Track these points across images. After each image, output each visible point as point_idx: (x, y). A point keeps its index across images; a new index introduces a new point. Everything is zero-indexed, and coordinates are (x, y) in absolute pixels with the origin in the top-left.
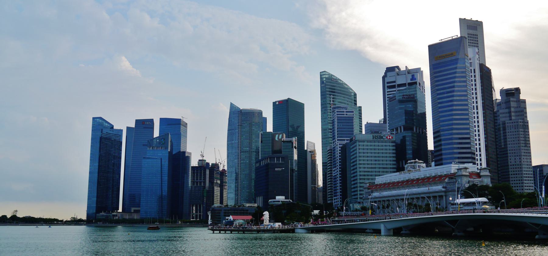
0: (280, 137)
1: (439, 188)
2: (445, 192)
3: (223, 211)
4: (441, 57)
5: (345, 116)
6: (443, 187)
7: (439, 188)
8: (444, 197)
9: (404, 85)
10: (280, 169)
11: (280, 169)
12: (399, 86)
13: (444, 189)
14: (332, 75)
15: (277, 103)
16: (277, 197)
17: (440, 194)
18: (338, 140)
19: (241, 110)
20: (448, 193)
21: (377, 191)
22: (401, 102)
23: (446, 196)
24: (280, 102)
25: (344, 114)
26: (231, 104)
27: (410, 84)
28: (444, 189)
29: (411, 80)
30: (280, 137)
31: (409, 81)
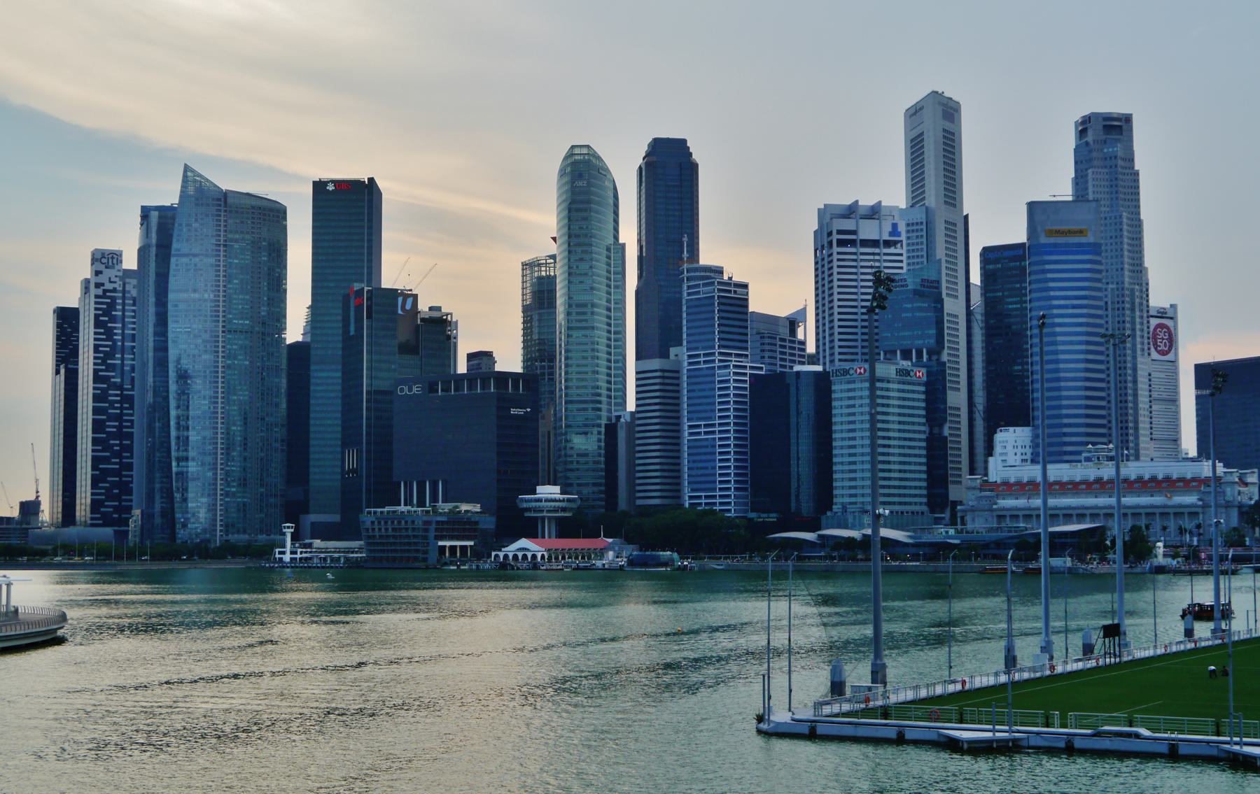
0: (408, 306)
1: (1190, 499)
2: (1203, 507)
3: (434, 526)
4: (1059, 233)
6: (1200, 500)
7: (1190, 499)
9: (875, 243)
10: (520, 412)
11: (520, 412)
12: (865, 243)
15: (331, 187)
16: (540, 489)
17: (1193, 510)
18: (720, 354)
19: (226, 195)
22: (916, 292)
24: (339, 184)
25: (730, 291)
26: (187, 169)
27: (888, 244)
29: (891, 234)
30: (408, 306)
31: (886, 237)
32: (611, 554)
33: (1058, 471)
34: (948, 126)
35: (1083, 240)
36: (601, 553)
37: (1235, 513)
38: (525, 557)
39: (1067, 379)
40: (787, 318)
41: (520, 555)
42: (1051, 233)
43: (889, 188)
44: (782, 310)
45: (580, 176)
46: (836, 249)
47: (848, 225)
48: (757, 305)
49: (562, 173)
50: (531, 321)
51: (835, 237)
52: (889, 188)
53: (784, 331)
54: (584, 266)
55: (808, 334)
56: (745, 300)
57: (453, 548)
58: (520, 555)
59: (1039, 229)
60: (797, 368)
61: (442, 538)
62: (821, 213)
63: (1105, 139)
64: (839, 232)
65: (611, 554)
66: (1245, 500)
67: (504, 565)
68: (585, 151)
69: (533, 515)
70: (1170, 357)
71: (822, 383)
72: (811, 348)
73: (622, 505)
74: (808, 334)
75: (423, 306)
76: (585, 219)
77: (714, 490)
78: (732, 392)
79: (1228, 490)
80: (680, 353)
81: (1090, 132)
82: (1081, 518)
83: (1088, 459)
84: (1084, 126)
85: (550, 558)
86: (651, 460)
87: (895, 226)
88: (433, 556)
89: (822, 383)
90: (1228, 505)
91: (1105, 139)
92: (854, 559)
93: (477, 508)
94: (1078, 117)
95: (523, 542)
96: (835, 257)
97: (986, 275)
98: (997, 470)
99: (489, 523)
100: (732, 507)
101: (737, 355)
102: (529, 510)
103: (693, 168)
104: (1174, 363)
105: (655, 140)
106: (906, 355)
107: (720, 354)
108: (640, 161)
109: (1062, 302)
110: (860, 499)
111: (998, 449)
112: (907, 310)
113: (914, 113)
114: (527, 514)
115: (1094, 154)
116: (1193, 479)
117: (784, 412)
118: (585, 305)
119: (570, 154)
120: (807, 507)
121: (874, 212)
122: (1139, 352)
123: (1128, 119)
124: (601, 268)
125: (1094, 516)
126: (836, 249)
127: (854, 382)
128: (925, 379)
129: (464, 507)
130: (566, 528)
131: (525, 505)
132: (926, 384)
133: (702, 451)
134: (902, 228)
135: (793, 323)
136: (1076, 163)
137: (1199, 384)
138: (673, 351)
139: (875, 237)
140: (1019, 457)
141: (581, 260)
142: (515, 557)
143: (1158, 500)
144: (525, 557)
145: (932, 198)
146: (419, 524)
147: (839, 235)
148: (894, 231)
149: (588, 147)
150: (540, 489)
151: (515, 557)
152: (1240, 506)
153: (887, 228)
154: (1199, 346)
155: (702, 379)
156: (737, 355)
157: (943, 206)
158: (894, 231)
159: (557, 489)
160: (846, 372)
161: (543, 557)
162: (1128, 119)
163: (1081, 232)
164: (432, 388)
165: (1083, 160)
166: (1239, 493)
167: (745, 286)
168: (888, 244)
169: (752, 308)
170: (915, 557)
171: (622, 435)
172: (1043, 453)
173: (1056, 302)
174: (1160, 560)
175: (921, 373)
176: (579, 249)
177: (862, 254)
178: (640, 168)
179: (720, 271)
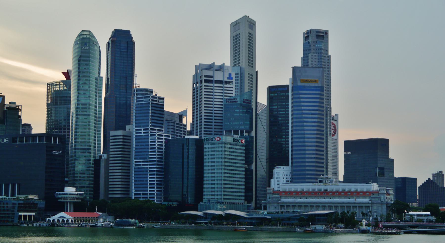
2: (371, 204)
3: (17, 206)
4: (306, 81)
5: (157, 103)
6: (370, 201)
7: (366, 200)
8: (370, 208)
9: (221, 82)
12: (217, 82)
13: (370, 202)
14: (94, 37)
16: (66, 189)
18: (151, 129)
20: (373, 205)
21: (286, 197)
22: (241, 105)
23: (371, 206)
25: (156, 101)
27: (227, 82)
28: (370, 202)
29: (228, 78)
31: (226, 79)
32: (101, 220)
33: (299, 187)
34: (251, 31)
35: (316, 85)
36: (97, 219)
37: (385, 207)
38: (63, 221)
39: (308, 146)
40: (179, 114)
41: (61, 219)
42: (302, 81)
43: (223, 57)
44: (177, 111)
45: (86, 45)
46: (204, 84)
47: (210, 73)
48: (167, 108)
49: (76, 43)
50: (51, 110)
51: (204, 78)
52: (223, 57)
53: (177, 120)
54: (86, 87)
55: (188, 121)
56: (162, 106)
57: (25, 216)
58: (61, 219)
59: (298, 79)
60: (187, 137)
61: (20, 212)
62: (197, 67)
63: (316, 41)
64: (206, 76)
65: (101, 220)
66: (389, 201)
67: (53, 224)
68: (88, 33)
69: (63, 201)
70: (335, 137)
71: (199, 144)
72: (188, 128)
73: (102, 197)
74: (188, 121)
75: (7, 102)
76: (87, 65)
77: (147, 191)
78: (156, 146)
79: (382, 197)
80: (132, 128)
81: (310, 38)
82: (324, 208)
83: (321, 182)
84: (307, 35)
85: (75, 221)
86: (117, 176)
87: (230, 75)
88: (16, 220)
89: (199, 144)
90: (382, 203)
91: (316, 41)
92: (223, 225)
93: (36, 197)
94: (305, 30)
95: (62, 214)
96: (204, 87)
97: (270, 99)
98: (274, 185)
99: (42, 204)
100: (155, 199)
101: (158, 130)
102: (61, 198)
103: (133, 44)
104: (336, 140)
105: (129, 32)
106: (236, 132)
107: (151, 129)
108: (108, 40)
109: (307, 112)
110: (216, 197)
111: (275, 176)
112: (237, 113)
113: (235, 25)
114: (59, 201)
115: (312, 47)
116: (367, 192)
117: (183, 157)
118: (86, 104)
119: (81, 34)
120: (190, 200)
121: (221, 68)
122: (328, 135)
123: (326, 33)
124: (93, 87)
125: (330, 207)
126: (204, 84)
127: (214, 144)
128: (245, 144)
129: (30, 197)
130: (79, 206)
131: (59, 196)
132: (245, 146)
133: (140, 173)
134: (233, 76)
135: (181, 116)
136: (304, 51)
137: (346, 150)
138: (128, 127)
139: (222, 79)
140: (285, 180)
141: (85, 83)
142: (58, 221)
143: (352, 200)
144: (63, 221)
145: (243, 63)
146: (10, 205)
147: (205, 78)
148: (230, 77)
149: (90, 31)
150: (66, 189)
151: (58, 221)
152: (387, 204)
153: (227, 76)
154: (347, 132)
155: (142, 141)
156: (158, 130)
157: (248, 67)
158: (230, 77)
159: (74, 189)
160: (211, 139)
161: (72, 221)
162: (326, 33)
163: (316, 81)
164: (14, 140)
165: (307, 50)
166: (387, 198)
167: (163, 99)
168: (227, 82)
169: (166, 109)
170: (251, 224)
171: (102, 165)
172: (295, 178)
173: (304, 112)
174: (364, 227)
175: (243, 141)
176: (84, 79)
177: (215, 87)
178: (108, 43)
179: (151, 92)
